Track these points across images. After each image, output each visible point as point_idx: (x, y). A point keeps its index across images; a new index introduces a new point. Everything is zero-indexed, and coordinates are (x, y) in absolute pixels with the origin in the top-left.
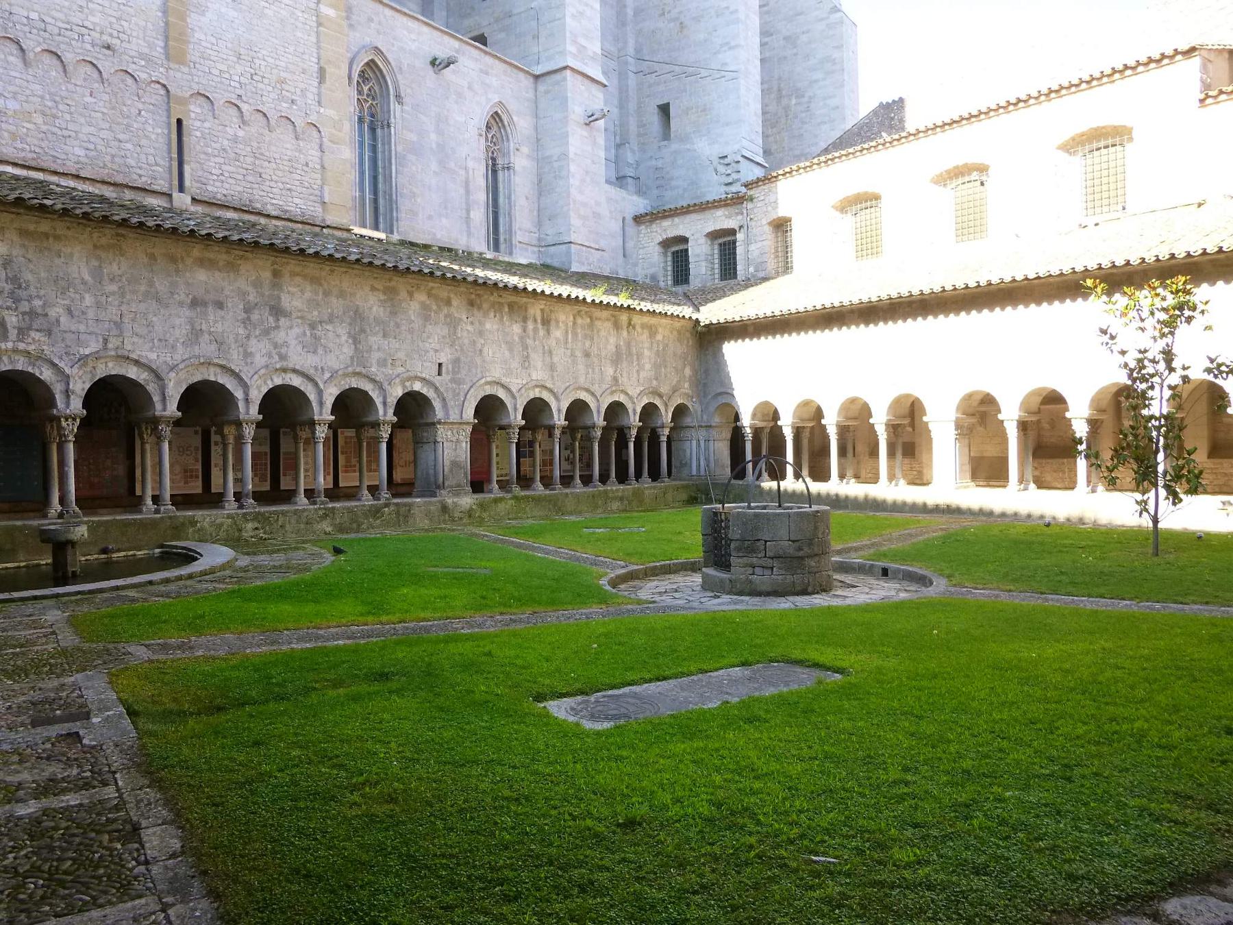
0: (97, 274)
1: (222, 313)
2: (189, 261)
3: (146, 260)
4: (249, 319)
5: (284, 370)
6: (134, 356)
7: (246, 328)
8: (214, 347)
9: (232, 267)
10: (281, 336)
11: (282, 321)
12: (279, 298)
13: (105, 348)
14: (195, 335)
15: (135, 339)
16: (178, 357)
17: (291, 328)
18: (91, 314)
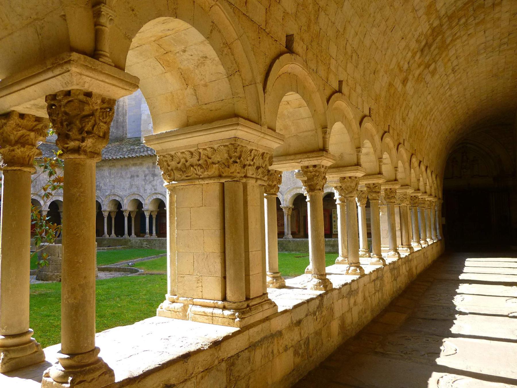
0: (110, 174)
1: (138, 178)
2: (130, 165)
3: (120, 167)
4: (145, 179)
5: (156, 194)
6: (116, 194)
7: (145, 182)
8: (136, 189)
9: (141, 164)
10: (154, 183)
11: (156, 178)
12: (154, 171)
13: (111, 193)
14: (131, 186)
15: (118, 189)
16: (127, 193)
17: (158, 180)
18: (108, 184)
